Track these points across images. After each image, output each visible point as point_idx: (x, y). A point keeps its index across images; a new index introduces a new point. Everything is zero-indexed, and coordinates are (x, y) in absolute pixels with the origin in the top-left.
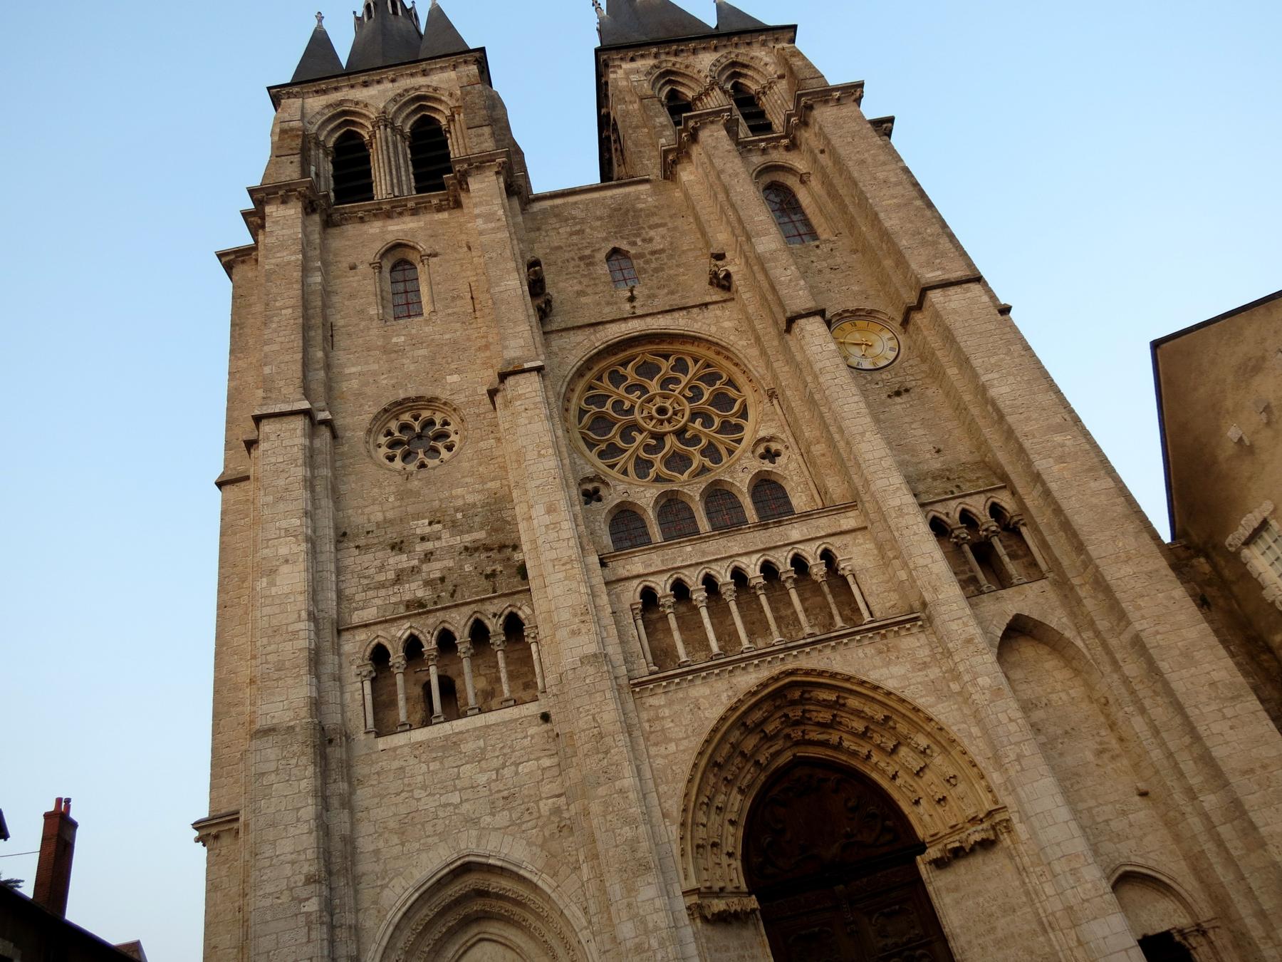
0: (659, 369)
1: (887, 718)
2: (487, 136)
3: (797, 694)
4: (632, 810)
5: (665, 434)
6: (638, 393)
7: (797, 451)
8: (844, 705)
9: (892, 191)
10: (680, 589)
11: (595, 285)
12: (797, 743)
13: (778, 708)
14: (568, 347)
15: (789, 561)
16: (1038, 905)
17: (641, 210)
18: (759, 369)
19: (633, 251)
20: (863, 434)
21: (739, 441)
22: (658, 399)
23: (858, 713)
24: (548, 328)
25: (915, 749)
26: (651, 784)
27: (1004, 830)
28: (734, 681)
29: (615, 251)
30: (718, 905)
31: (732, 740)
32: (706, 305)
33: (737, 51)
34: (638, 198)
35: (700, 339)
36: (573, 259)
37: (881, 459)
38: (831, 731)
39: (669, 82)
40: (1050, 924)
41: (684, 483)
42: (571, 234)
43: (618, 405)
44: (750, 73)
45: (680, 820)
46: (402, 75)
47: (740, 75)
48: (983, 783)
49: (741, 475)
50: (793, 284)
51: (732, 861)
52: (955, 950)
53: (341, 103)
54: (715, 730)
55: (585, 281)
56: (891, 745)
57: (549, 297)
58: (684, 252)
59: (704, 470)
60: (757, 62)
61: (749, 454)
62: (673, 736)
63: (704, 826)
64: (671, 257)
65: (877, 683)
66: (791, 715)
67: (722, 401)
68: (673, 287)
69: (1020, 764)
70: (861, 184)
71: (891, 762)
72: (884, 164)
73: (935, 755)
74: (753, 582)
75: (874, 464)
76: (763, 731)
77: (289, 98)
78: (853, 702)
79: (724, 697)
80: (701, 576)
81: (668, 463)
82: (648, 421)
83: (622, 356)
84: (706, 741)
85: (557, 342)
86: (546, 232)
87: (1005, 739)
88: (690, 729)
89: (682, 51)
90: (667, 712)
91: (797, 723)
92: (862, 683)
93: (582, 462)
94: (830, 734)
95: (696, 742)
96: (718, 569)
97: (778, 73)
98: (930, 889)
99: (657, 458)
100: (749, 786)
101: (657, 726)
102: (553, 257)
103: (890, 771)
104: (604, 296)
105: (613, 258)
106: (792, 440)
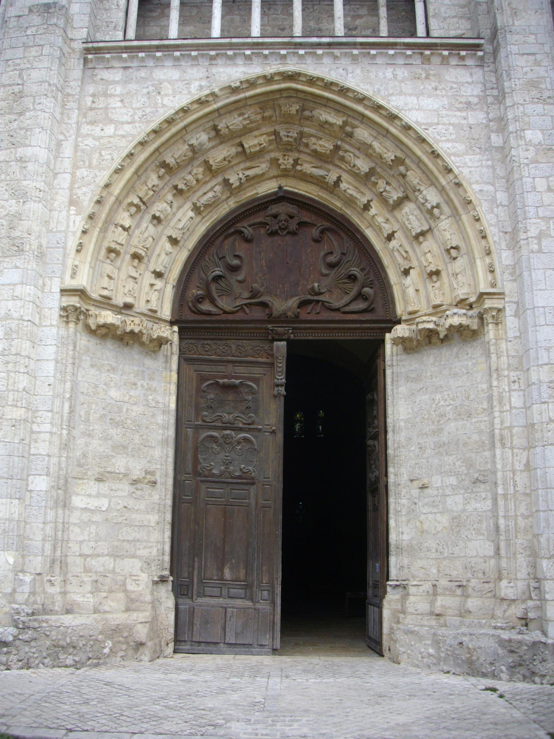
1: (398, 161)
4: (25, 183)
8: (350, 135)
16: (497, 414)
25: (421, 206)
26: (67, 164)
27: (490, 320)
28: (214, 70)
31: (193, 141)
38: (330, 167)
40: (502, 439)
45: (89, 211)
48: (488, 260)
51: (159, 284)
52: (390, 443)
54: (170, 121)
56: (395, 196)
62: (115, 117)
63: (124, 229)
65: (395, 111)
66: (282, 133)
69: (539, 244)
71: (392, 220)
73: (442, 217)
76: (242, 145)
79: (195, 86)
84: (155, 132)
88: (140, 113)
91: (288, 148)
92: (378, 108)
94: (329, 171)
98: (388, 372)
101: (101, 103)
103: (387, 229)
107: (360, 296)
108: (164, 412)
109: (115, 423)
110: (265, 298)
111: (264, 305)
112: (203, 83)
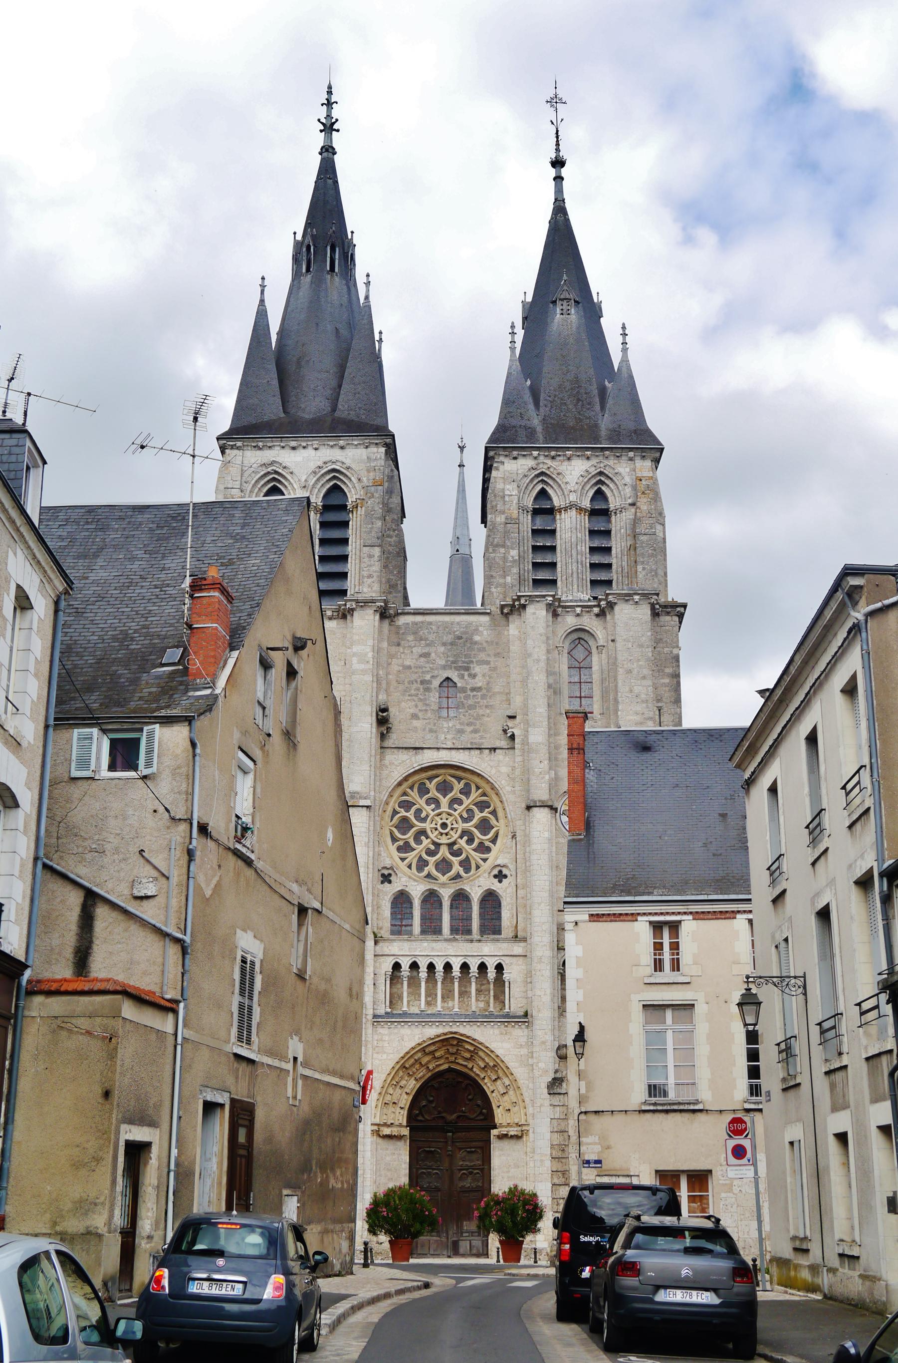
0: (452, 789)
1: (495, 1066)
2: (376, 558)
3: (455, 1042)
5: (441, 844)
6: (433, 806)
7: (515, 882)
9: (639, 708)
10: (414, 966)
11: (426, 710)
12: (452, 1062)
13: (445, 1046)
14: (396, 763)
15: (477, 966)
17: (476, 643)
18: (512, 814)
19: (459, 685)
20: (539, 904)
21: (485, 860)
22: (444, 816)
23: (483, 1060)
24: (386, 744)
28: (424, 1030)
29: (448, 679)
30: (387, 1131)
31: (416, 1058)
32: (495, 749)
33: (606, 462)
34: (477, 630)
35: (483, 777)
36: (416, 682)
37: (543, 923)
39: (542, 481)
41: (443, 885)
42: (421, 656)
43: (419, 811)
44: (611, 485)
46: (324, 444)
47: (603, 483)
49: (477, 888)
50: (542, 776)
51: (402, 1111)
53: (273, 463)
54: (407, 1053)
55: (420, 704)
57: (390, 726)
58: (494, 694)
59: (458, 876)
60: (620, 477)
61: (486, 875)
64: (483, 697)
67: (484, 826)
68: (477, 727)
70: (619, 694)
72: (644, 678)
74: (453, 975)
75: (538, 926)
77: (232, 448)
78: (481, 1054)
79: (417, 1037)
80: (428, 963)
81: (437, 866)
82: (434, 830)
83: (430, 773)
85: (390, 757)
86: (404, 648)
87: (538, 1096)
88: (396, 1050)
89: (559, 455)
90: (387, 1038)
92: (487, 1047)
93: (385, 855)
95: (397, 1057)
96: (437, 960)
97: (630, 501)
99: (432, 860)
100: (420, 1078)
101: (380, 1044)
102: (402, 676)
103: (492, 1088)
104: (429, 723)
105: (445, 684)
106: (514, 873)
107: (481, 1113)
108: (405, 1163)
109: (389, 1170)
110: (444, 1115)
111: (443, 1117)
112: (420, 1036)
